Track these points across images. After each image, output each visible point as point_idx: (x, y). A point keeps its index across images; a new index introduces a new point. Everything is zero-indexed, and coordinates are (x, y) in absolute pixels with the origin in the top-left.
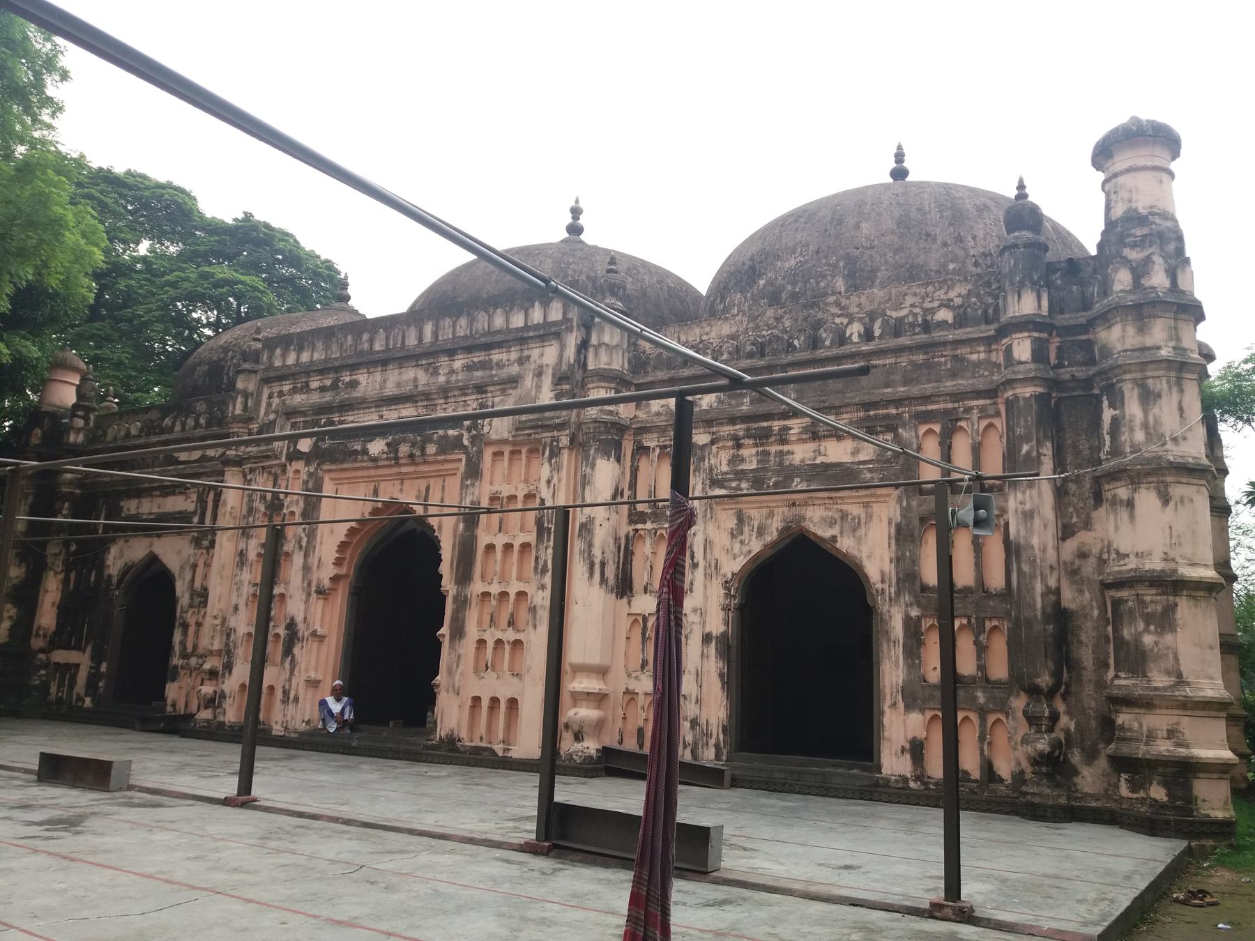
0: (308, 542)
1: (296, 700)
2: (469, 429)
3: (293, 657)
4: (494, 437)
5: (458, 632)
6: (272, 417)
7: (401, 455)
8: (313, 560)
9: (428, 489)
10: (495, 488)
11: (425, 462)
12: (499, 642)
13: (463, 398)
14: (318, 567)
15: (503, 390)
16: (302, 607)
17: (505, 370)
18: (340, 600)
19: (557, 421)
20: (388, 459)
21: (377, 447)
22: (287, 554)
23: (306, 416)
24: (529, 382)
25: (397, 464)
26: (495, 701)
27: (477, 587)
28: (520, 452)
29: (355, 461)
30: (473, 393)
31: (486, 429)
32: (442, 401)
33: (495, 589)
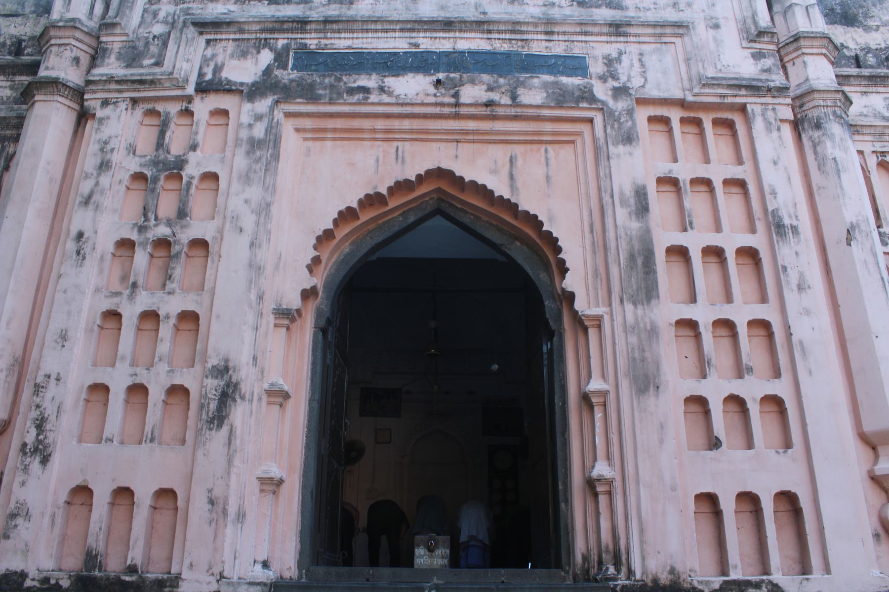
0: (258, 224)
1: (241, 516)
2: (603, 78)
3: (231, 431)
4: (655, 94)
5: (646, 382)
6: (158, 29)
7: (463, 100)
8: (265, 255)
9: (512, 161)
10: (665, 167)
11: (516, 118)
12: (736, 402)
13: (583, 38)
14: (277, 268)
15: (661, 35)
16: (248, 336)
17: (649, 14)
18: (306, 332)
19: (772, 84)
20: (436, 104)
21: (412, 86)
22: (200, 244)
23: (242, 31)
24: (702, 32)
25: (457, 116)
26: (749, 501)
27: (668, 309)
28: (698, 123)
29: (364, 102)
30: (601, 34)
31: (637, 82)
32: (543, 37)
33: (704, 314)
